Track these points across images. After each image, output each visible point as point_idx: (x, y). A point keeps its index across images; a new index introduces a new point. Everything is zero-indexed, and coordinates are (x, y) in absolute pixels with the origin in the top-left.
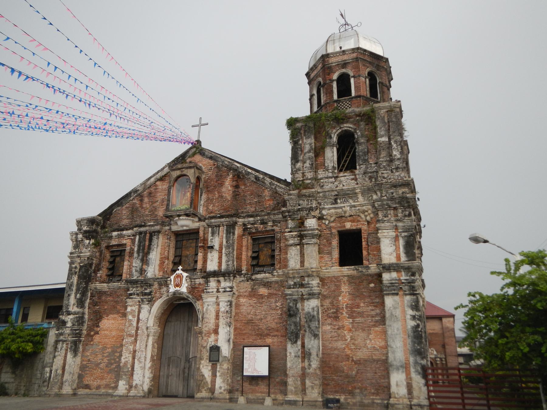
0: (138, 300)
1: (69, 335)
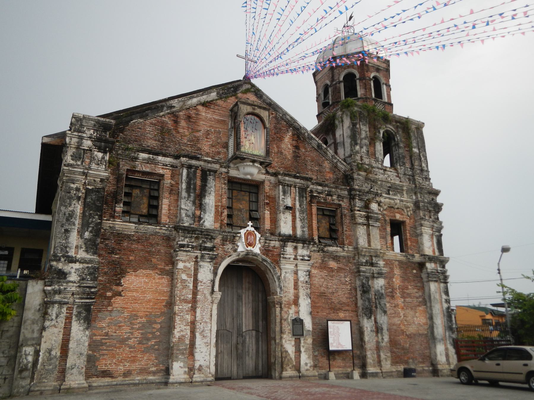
0: (196, 254)
1: (73, 294)
